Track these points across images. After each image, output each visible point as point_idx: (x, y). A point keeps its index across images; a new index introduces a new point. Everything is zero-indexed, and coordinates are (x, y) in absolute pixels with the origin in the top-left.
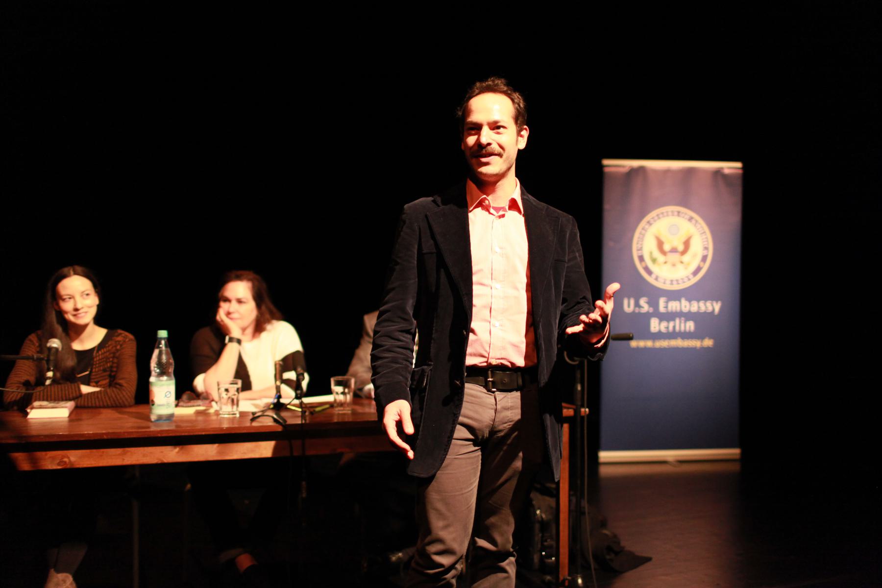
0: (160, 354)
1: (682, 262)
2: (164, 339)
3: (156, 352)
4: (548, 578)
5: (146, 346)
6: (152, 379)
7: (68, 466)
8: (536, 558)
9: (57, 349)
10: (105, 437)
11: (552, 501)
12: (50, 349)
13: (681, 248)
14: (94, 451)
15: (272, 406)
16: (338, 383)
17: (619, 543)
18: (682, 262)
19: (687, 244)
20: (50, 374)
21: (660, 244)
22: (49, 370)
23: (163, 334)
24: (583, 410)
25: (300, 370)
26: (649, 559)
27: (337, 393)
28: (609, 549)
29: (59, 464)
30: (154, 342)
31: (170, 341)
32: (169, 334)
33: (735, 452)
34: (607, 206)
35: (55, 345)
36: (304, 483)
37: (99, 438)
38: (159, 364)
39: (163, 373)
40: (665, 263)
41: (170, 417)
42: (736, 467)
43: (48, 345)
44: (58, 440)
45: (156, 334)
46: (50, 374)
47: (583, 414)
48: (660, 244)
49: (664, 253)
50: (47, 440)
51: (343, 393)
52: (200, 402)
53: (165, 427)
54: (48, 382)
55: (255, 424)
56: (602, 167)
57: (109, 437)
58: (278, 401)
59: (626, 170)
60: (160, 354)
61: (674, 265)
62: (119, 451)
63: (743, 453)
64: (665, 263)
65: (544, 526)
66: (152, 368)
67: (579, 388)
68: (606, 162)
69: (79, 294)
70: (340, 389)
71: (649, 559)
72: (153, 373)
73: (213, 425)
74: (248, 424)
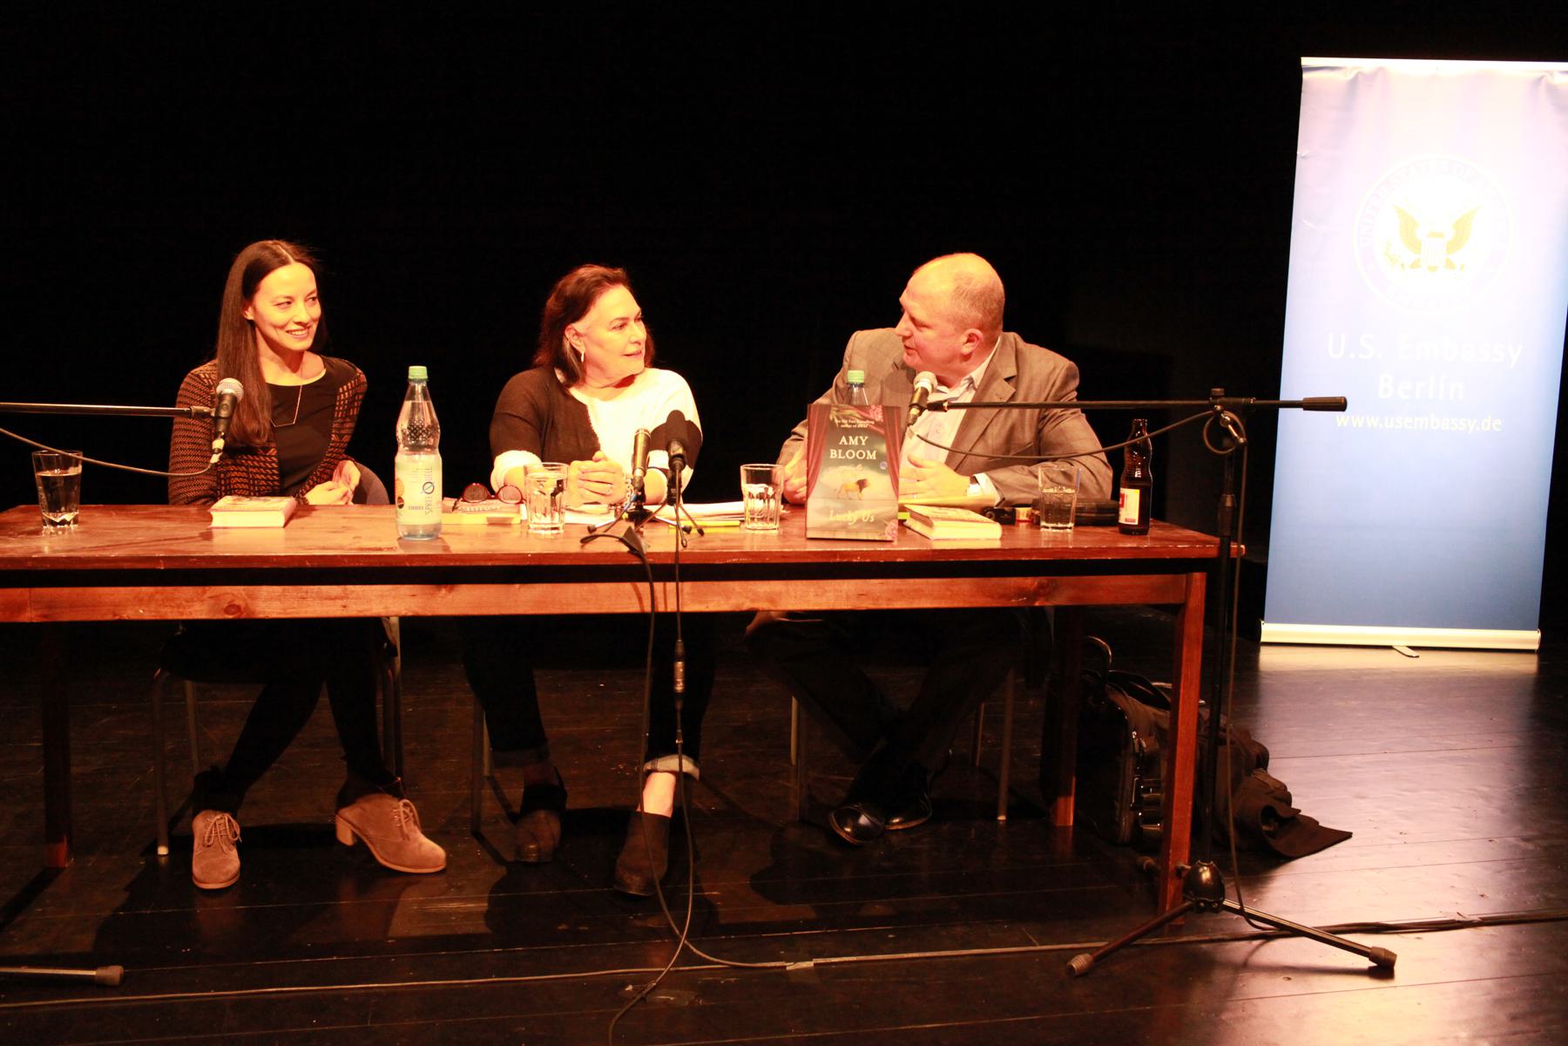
0: (416, 412)
1: (1450, 265)
2: (420, 381)
3: (407, 405)
4: (1149, 860)
5: (390, 393)
6: (403, 459)
7: (244, 616)
8: (1125, 822)
9: (234, 398)
11: (1163, 715)
12: (221, 397)
14: (290, 588)
15: (626, 515)
16: (755, 478)
17: (1287, 799)
18: (1450, 265)
22: (216, 437)
23: (418, 372)
24: (1234, 546)
25: (677, 449)
26: (1347, 836)
27: (751, 496)
28: (1269, 813)
29: (226, 611)
30: (401, 389)
31: (434, 389)
32: (429, 374)
34: (1302, 151)
35: (228, 391)
36: (680, 664)
38: (414, 431)
39: (416, 448)
40: (1415, 265)
41: (434, 532)
42: (1530, 665)
45: (406, 373)
46: (219, 444)
47: (1233, 555)
50: (204, 565)
51: (761, 497)
52: (495, 503)
53: (422, 548)
54: (215, 459)
55: (593, 548)
56: (1298, 71)
58: (639, 507)
59: (1350, 76)
60: (416, 412)
63: (1543, 641)
64: (1415, 265)
65: (1147, 764)
66: (399, 435)
67: (1229, 504)
68: (1306, 61)
69: (288, 294)
70: (758, 488)
71: (1347, 836)
72: (401, 447)
73: (513, 544)
74: (575, 547)
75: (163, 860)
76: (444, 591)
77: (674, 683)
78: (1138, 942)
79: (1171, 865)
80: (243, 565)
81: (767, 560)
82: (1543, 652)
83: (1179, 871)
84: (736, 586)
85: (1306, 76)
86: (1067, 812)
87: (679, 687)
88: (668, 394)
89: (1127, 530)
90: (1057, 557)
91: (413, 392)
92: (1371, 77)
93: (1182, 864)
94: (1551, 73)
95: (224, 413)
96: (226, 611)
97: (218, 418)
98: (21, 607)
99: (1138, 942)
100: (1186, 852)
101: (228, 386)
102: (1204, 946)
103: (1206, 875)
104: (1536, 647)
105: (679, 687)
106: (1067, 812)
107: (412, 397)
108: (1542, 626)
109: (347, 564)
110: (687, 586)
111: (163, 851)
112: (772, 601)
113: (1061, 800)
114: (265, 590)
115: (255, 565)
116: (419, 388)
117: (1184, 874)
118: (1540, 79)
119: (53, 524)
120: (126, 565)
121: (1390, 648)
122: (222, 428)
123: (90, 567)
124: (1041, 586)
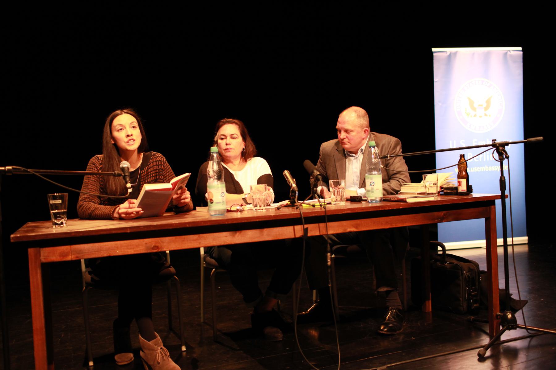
1: (486, 115)
7: (159, 251)
10: (188, 226)
13: (485, 105)
14: (178, 237)
18: (486, 115)
19: (488, 102)
20: (129, 185)
21: (471, 103)
22: (127, 183)
33: (525, 239)
34: (436, 79)
35: (125, 166)
37: (183, 226)
40: (475, 116)
42: (525, 249)
43: (121, 166)
44: (153, 229)
45: (210, 150)
48: (471, 103)
49: (474, 109)
56: (432, 53)
57: (191, 226)
59: (448, 54)
61: (481, 117)
62: (195, 237)
63: (529, 240)
64: (475, 116)
68: (434, 50)
75: (91, 368)
76: (238, 234)
77: (327, 262)
78: (496, 343)
79: (494, 315)
80: (159, 229)
81: (357, 211)
82: (530, 243)
83: (497, 315)
84: (345, 223)
85: (434, 54)
86: (429, 306)
87: (329, 264)
88: (260, 166)
89: (462, 194)
90: (451, 203)
91: (213, 156)
92: (456, 53)
93: (499, 313)
94: (509, 51)
95: (127, 174)
96: (153, 249)
97: (125, 176)
98: (67, 255)
99: (496, 343)
100: (498, 309)
101: (124, 164)
102: (505, 344)
103: (510, 316)
104: (527, 242)
105: (329, 264)
106: (429, 306)
107: (212, 159)
108: (528, 235)
109: (203, 224)
110: (330, 224)
111: (91, 364)
112: (356, 227)
113: (427, 302)
114: (166, 239)
115: (166, 228)
116: (215, 155)
117: (499, 317)
118: (506, 53)
119: (56, 224)
120: (114, 232)
121: (480, 248)
122: (128, 179)
123: (99, 234)
124: (444, 215)
